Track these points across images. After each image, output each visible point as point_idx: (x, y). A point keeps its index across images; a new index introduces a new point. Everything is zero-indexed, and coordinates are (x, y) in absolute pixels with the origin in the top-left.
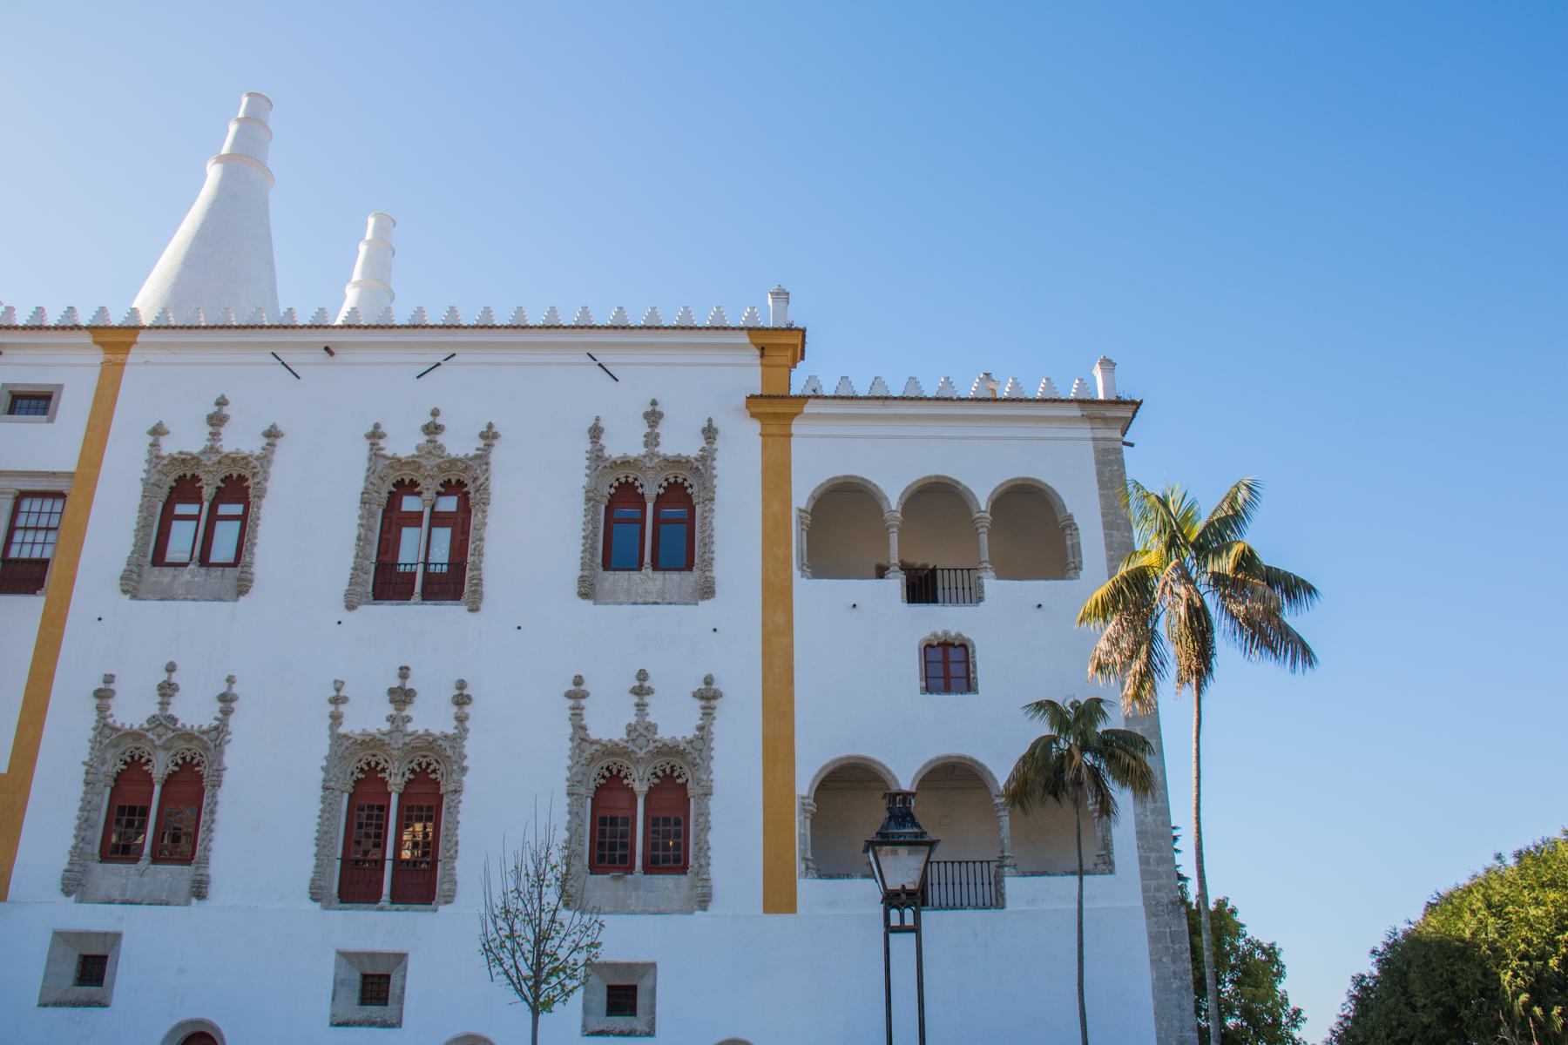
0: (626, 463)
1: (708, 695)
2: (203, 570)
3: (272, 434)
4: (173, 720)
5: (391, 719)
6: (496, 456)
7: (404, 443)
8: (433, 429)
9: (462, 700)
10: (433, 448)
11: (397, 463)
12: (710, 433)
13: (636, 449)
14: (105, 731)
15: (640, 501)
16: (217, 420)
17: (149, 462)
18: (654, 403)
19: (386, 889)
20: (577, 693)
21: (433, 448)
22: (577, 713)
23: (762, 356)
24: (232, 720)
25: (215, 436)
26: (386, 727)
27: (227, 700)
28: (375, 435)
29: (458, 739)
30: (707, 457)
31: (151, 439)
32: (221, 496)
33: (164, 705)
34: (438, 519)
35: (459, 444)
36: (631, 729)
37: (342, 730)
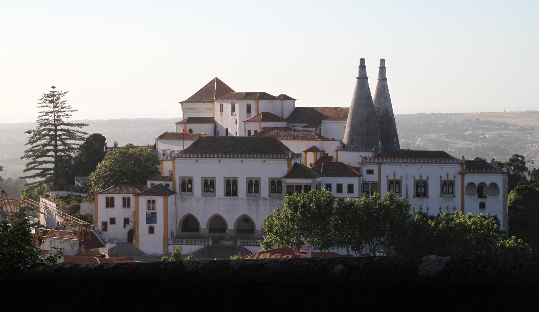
0: (445, 181)
3: (401, 177)
6: (429, 180)
7: (418, 178)
8: (421, 176)
9: (428, 209)
10: (421, 179)
12: (454, 177)
15: (446, 185)
16: (394, 175)
21: (421, 179)
28: (414, 177)
30: (454, 180)
32: (396, 184)
34: (423, 186)
35: (424, 178)
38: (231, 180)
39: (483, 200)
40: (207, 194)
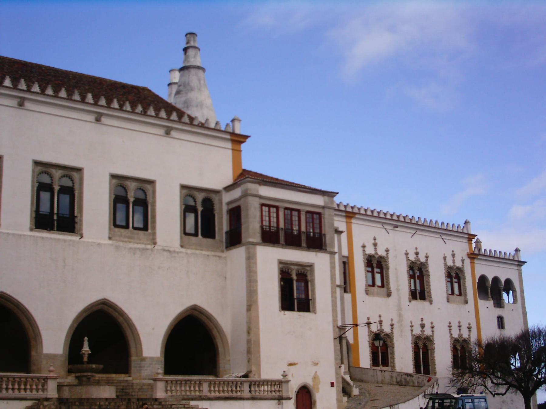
1: (469, 328)
2: (379, 288)
3: (387, 251)
4: (383, 330)
5: (421, 331)
7: (412, 257)
8: (417, 254)
9: (432, 328)
11: (413, 263)
12: (463, 261)
13: (452, 264)
14: (370, 332)
16: (375, 245)
17: (364, 255)
18: (453, 251)
19: (422, 372)
20: (450, 327)
21: (418, 260)
22: (450, 330)
23: (468, 241)
24: (394, 330)
25: (376, 249)
26: (421, 333)
27: (392, 325)
28: (407, 254)
29: (432, 336)
31: (362, 249)
33: (381, 326)
36: (459, 335)
37: (413, 333)
39: (498, 312)
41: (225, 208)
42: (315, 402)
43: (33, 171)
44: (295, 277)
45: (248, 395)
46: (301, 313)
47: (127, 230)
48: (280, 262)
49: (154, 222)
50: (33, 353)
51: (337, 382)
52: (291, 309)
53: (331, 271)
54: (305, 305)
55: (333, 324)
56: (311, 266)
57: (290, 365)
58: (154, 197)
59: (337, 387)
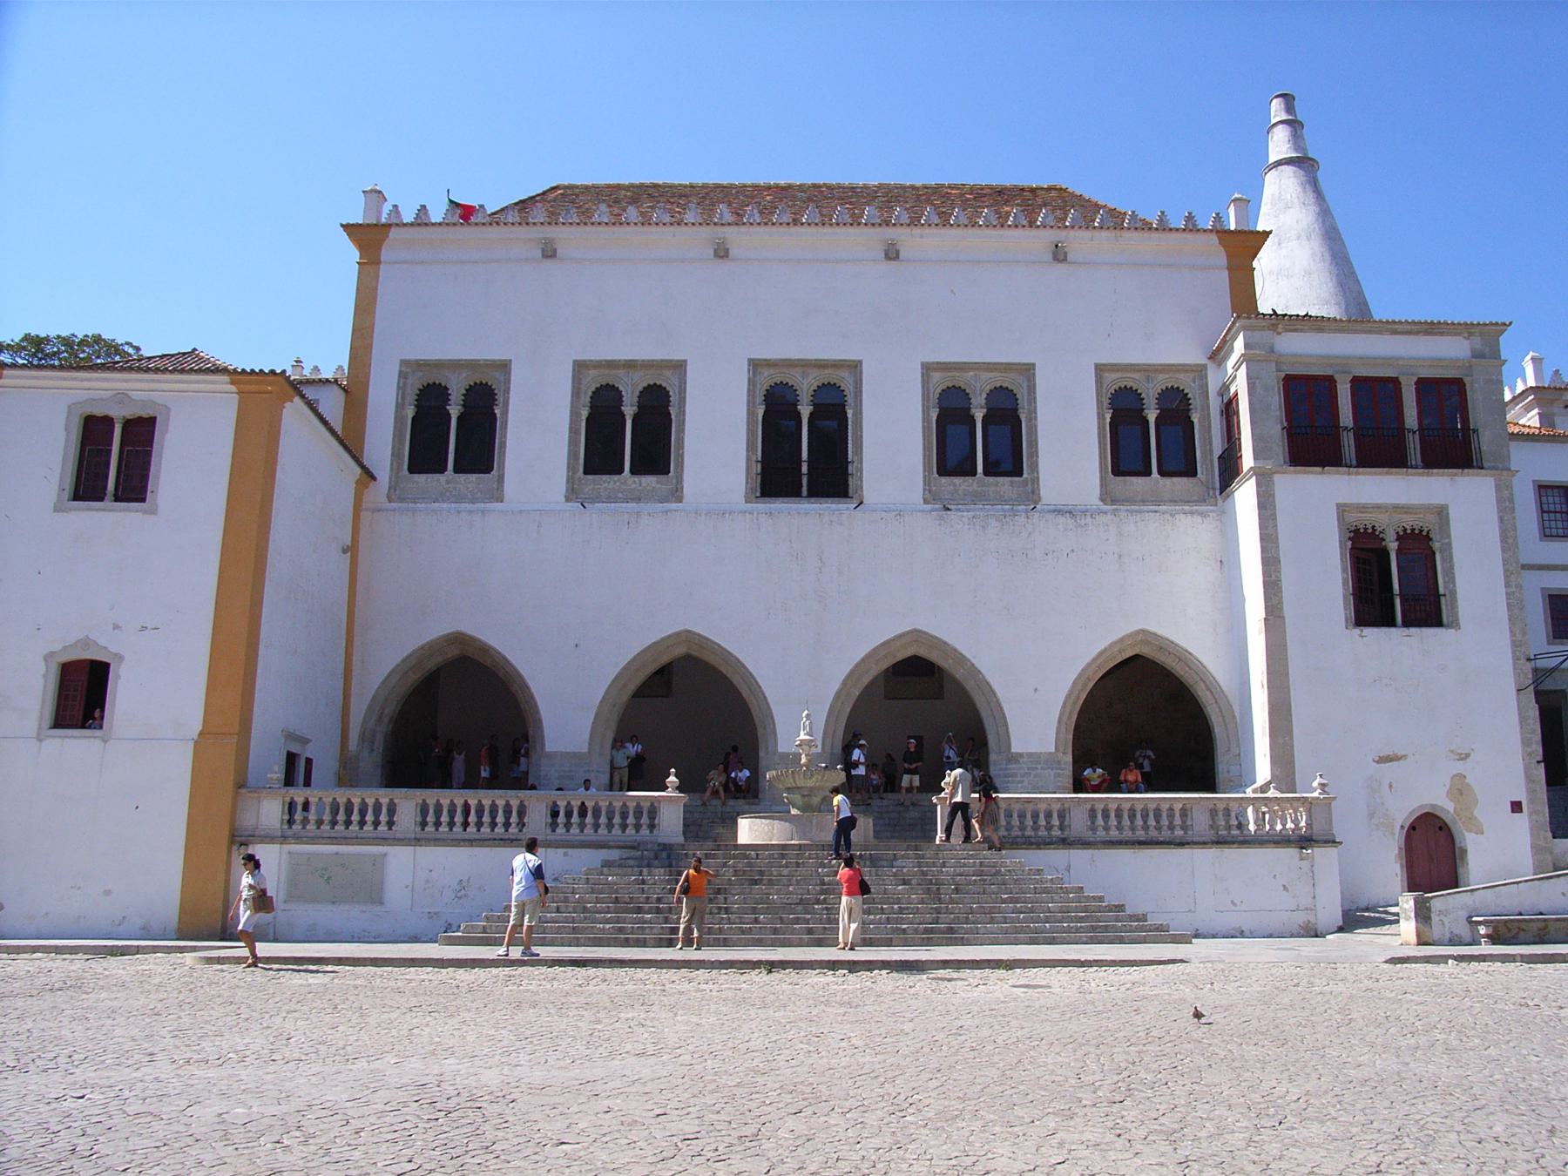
38: (806, 386)
40: (607, 482)
41: (1215, 405)
42: (1464, 852)
43: (751, 382)
44: (1393, 546)
45: (1210, 835)
46: (1413, 630)
47: (970, 479)
48: (1342, 510)
49: (1034, 454)
50: (762, 754)
51: (1531, 801)
52: (1389, 622)
53: (1501, 520)
54: (1427, 610)
55: (1514, 652)
56: (1442, 512)
57: (1383, 760)
58: (1032, 399)
59: (1530, 815)
